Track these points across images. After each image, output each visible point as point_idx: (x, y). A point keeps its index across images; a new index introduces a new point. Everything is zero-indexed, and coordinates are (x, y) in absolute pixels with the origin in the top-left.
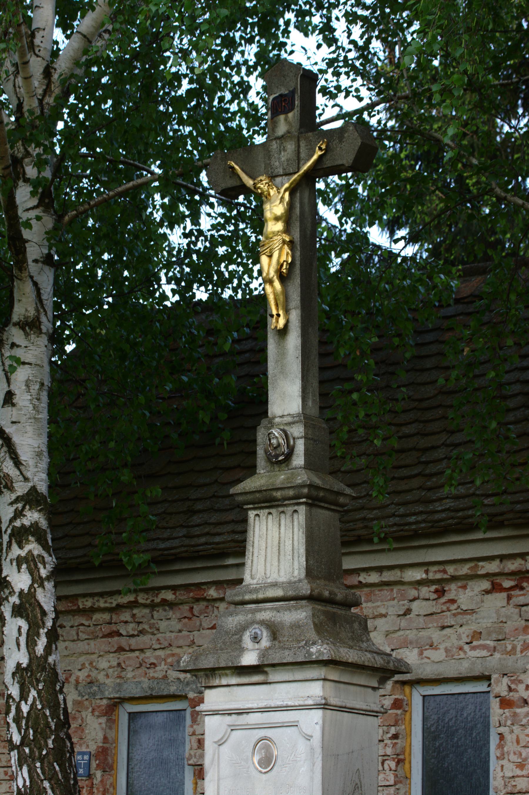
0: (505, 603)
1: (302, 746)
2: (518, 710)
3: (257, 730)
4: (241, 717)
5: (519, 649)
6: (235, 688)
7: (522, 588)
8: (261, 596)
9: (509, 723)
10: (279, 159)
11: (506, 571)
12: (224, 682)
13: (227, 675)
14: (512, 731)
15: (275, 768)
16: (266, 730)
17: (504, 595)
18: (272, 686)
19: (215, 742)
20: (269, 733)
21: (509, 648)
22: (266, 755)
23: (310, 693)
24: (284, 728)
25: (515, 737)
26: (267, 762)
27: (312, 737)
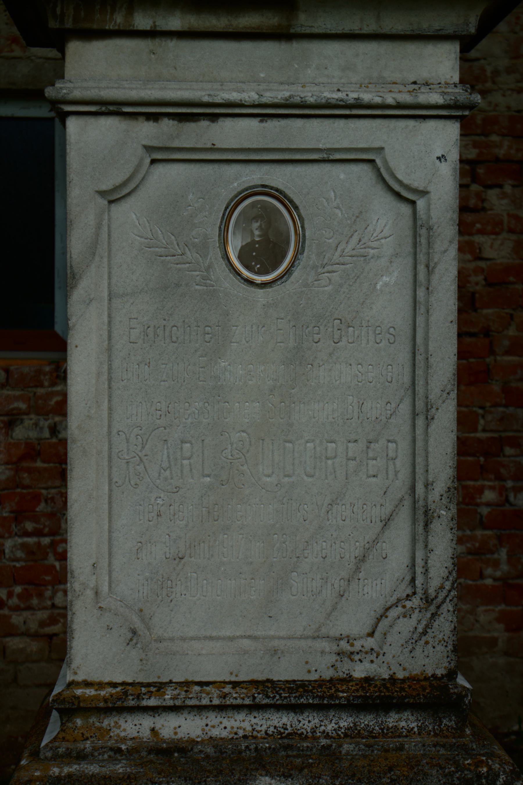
1: (385, 219)
3: (235, 168)
4: (191, 127)
6: (172, 44)
15: (297, 273)
16: (265, 168)
18: (296, 46)
19: (102, 193)
20: (278, 177)
22: (265, 235)
24: (327, 168)
26: (267, 254)
27: (424, 193)
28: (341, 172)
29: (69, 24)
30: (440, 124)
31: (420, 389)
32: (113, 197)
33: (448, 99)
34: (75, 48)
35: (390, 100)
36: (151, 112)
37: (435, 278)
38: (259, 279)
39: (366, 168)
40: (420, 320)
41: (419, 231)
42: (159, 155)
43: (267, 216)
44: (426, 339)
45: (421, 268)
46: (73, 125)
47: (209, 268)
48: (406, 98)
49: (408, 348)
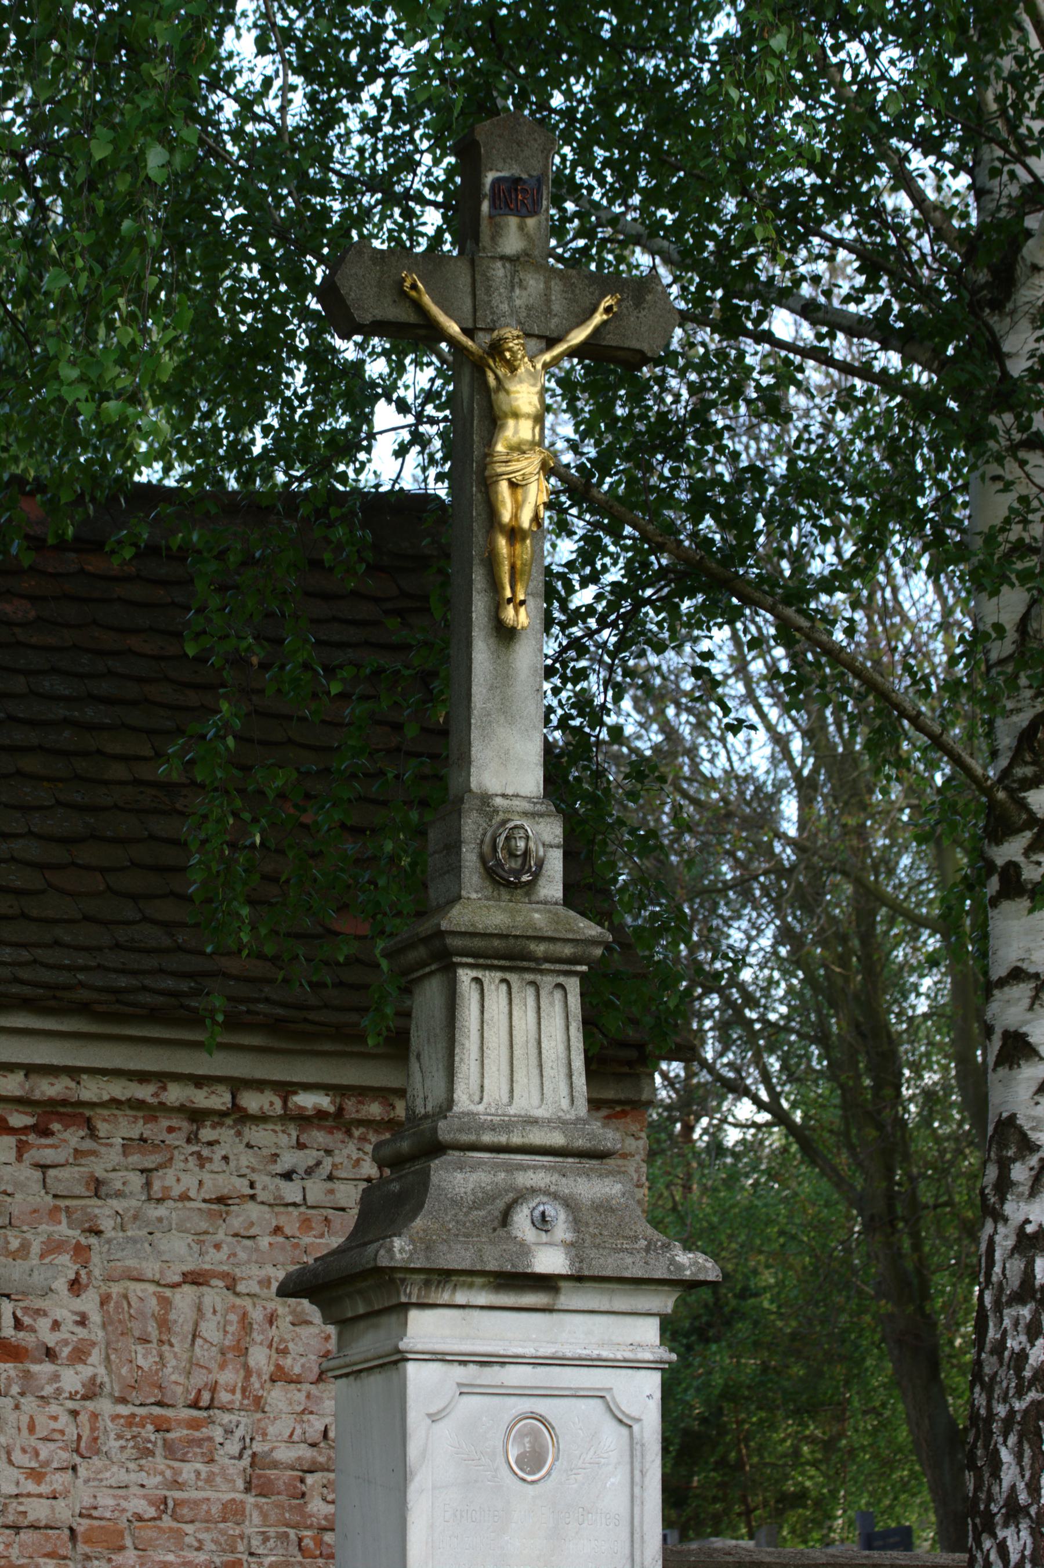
0: (12, 1156)
1: (612, 1436)
2: (35, 1368)
3: (514, 1399)
4: (487, 1370)
5: (36, 1248)
6: (476, 1313)
7: (46, 1133)
8: (516, 1140)
9: (15, 1390)
10: (510, 299)
11: (37, 1096)
12: (460, 1298)
13: (471, 1286)
14: (17, 1407)
15: (554, 1473)
16: (533, 1400)
17: (10, 1141)
18: (555, 1316)
19: (429, 1415)
20: (541, 1406)
21: (15, 1244)
22: (533, 1447)
23: (637, 1338)
24: (574, 1400)
25: (25, 1420)
26: (533, 1461)
27: (638, 1420)
28: (583, 1404)
29: (414, 1300)
30: (649, 1372)
31: (637, 1558)
32: (434, 1418)
33: (657, 1357)
34: (413, 1315)
35: (619, 1357)
36: (463, 1361)
37: (647, 1480)
38: (530, 1478)
39: (599, 1401)
40: (637, 1510)
41: (633, 1445)
42: (465, 1390)
43: (535, 1434)
44: (642, 1523)
45: (637, 1473)
46: (411, 1368)
47: (496, 1470)
48: (629, 1355)
49: (628, 1530)
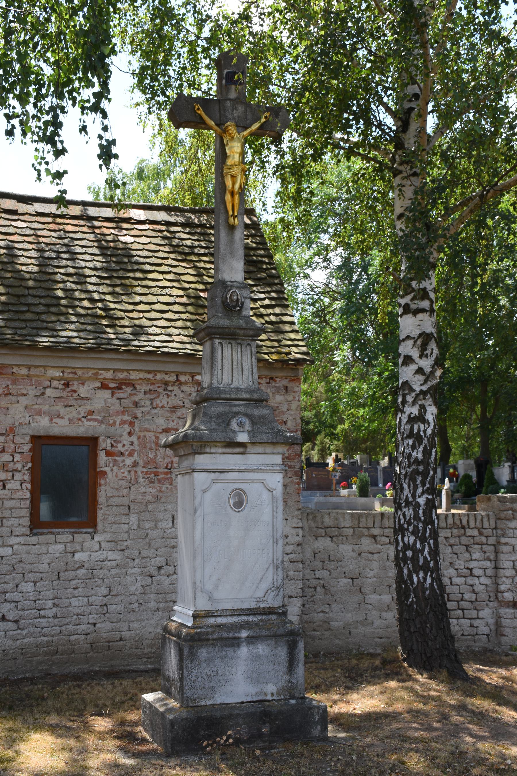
0: (110, 396)
1: (266, 496)
2: (117, 458)
5: (118, 423)
6: (218, 455)
7: (121, 389)
8: (233, 396)
9: (111, 465)
10: (232, 114)
11: (117, 378)
12: (213, 450)
13: (216, 446)
14: (112, 470)
17: (110, 391)
21: (111, 422)
25: (114, 474)
26: (239, 504)
28: (256, 485)
32: (204, 491)
42: (215, 481)
43: (239, 495)
